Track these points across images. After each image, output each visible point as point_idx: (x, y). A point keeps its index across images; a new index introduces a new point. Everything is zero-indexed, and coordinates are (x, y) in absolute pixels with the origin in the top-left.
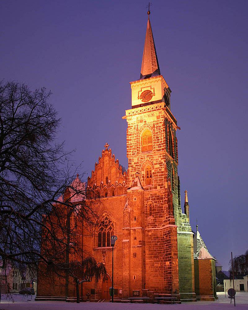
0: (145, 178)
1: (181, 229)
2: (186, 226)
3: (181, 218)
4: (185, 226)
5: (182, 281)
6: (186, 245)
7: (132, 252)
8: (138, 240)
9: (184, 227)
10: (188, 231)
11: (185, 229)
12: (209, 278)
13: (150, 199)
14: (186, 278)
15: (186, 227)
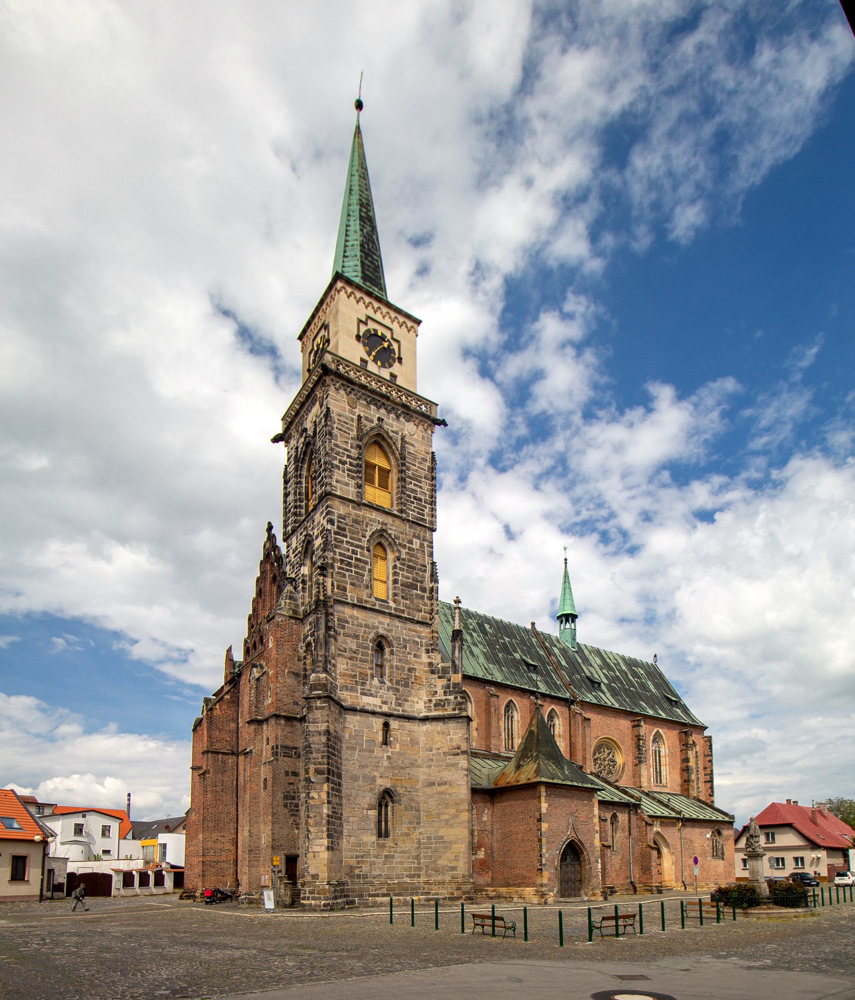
0: (309, 583)
1: (432, 705)
2: (448, 697)
3: (436, 676)
4: (444, 698)
5: (431, 848)
6: (445, 750)
7: (263, 777)
8: (271, 744)
9: (440, 700)
10: (454, 709)
11: (444, 706)
12: (536, 839)
13: (308, 636)
14: (442, 837)
15: (446, 700)
